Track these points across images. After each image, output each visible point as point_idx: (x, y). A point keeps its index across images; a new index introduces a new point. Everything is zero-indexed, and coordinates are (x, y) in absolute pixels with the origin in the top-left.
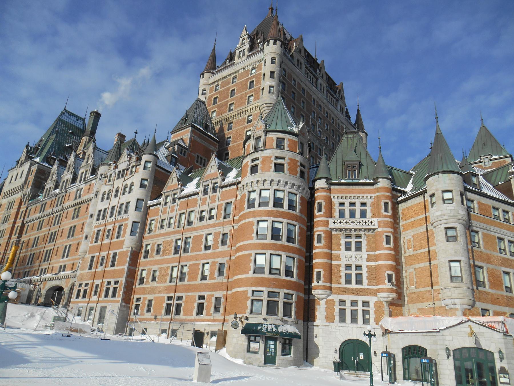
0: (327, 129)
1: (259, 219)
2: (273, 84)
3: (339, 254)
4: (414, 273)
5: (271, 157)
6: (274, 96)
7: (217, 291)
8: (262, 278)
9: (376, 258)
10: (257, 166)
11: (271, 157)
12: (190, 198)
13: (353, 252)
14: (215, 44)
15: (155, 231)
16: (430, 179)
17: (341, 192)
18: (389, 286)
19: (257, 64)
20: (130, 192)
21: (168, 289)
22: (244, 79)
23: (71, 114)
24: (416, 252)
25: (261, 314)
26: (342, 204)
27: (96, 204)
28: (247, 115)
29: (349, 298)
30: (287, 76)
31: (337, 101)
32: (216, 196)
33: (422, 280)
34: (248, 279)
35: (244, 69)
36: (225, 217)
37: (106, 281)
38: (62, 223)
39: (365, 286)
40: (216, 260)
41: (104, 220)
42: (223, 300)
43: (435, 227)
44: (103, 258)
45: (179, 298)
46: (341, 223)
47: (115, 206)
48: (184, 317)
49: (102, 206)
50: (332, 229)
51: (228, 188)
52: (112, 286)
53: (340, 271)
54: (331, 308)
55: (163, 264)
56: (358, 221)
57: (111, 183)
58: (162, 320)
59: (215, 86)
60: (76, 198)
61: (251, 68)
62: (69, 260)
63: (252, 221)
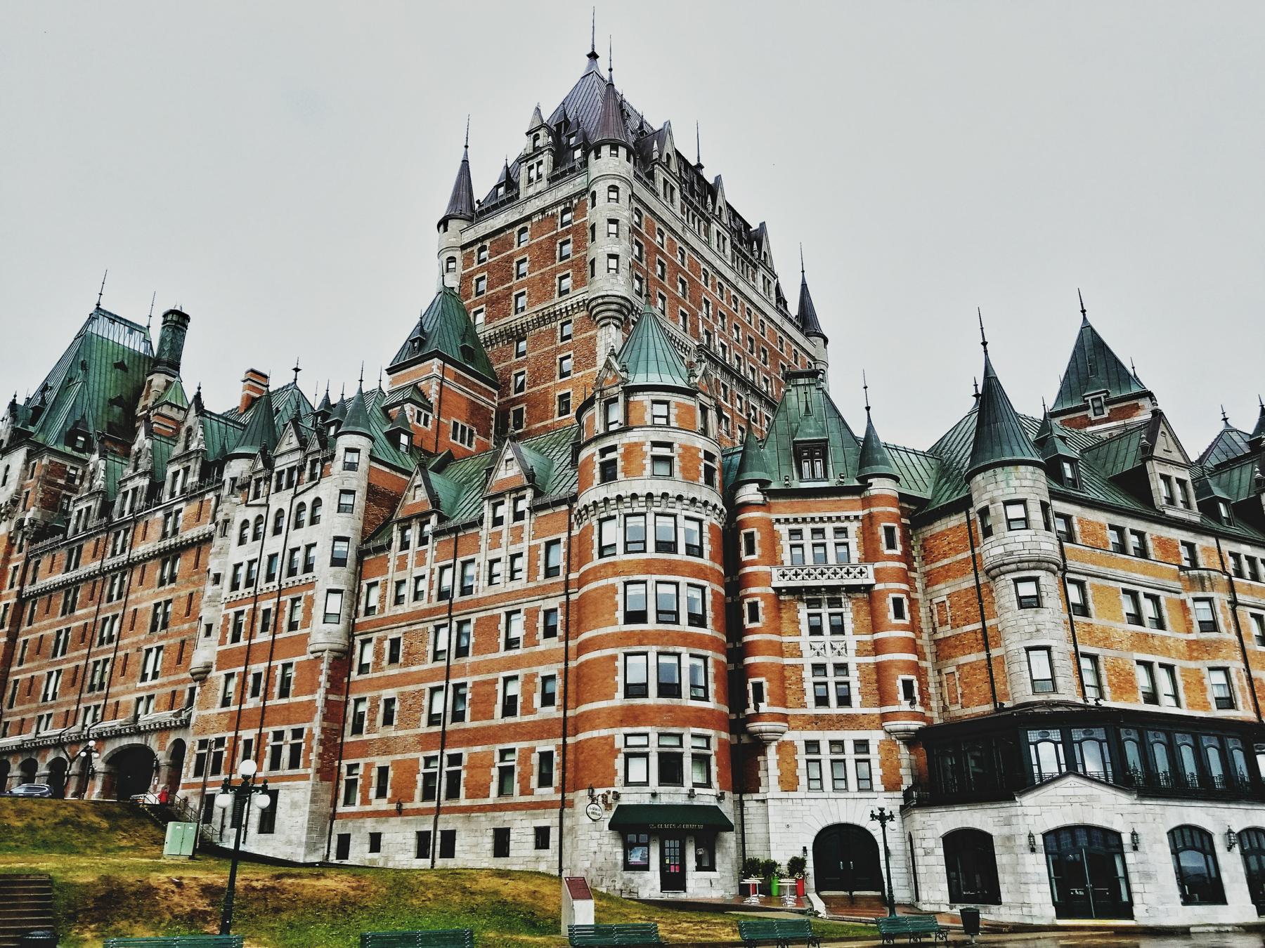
0: (738, 341)
1: (625, 579)
2: (615, 250)
3: (798, 643)
4: (957, 675)
5: (643, 444)
6: (619, 277)
7: (542, 738)
8: (644, 706)
9: (878, 647)
10: (614, 461)
11: (643, 444)
13: (827, 637)
14: (466, 147)
15: (383, 609)
16: (979, 477)
18: (905, 706)
20: (314, 520)
21: (425, 742)
23: (114, 319)
24: (958, 631)
25: (647, 784)
27: (222, 551)
28: (560, 322)
29: (824, 737)
30: (643, 226)
31: (755, 267)
32: (522, 527)
33: (974, 689)
34: (612, 710)
35: (543, 211)
36: (547, 575)
37: (269, 731)
38: (132, 597)
39: (856, 708)
41: (251, 589)
42: (557, 759)
43: (993, 578)
44: (257, 677)
45: (455, 760)
46: (796, 575)
47: (276, 555)
49: (242, 554)
50: (778, 590)
52: (286, 743)
53: (802, 680)
54: (789, 761)
55: (409, 684)
56: (832, 570)
57: (261, 500)
58: (418, 812)
59: (475, 251)
60: (164, 536)
62: (163, 685)
63: (613, 585)
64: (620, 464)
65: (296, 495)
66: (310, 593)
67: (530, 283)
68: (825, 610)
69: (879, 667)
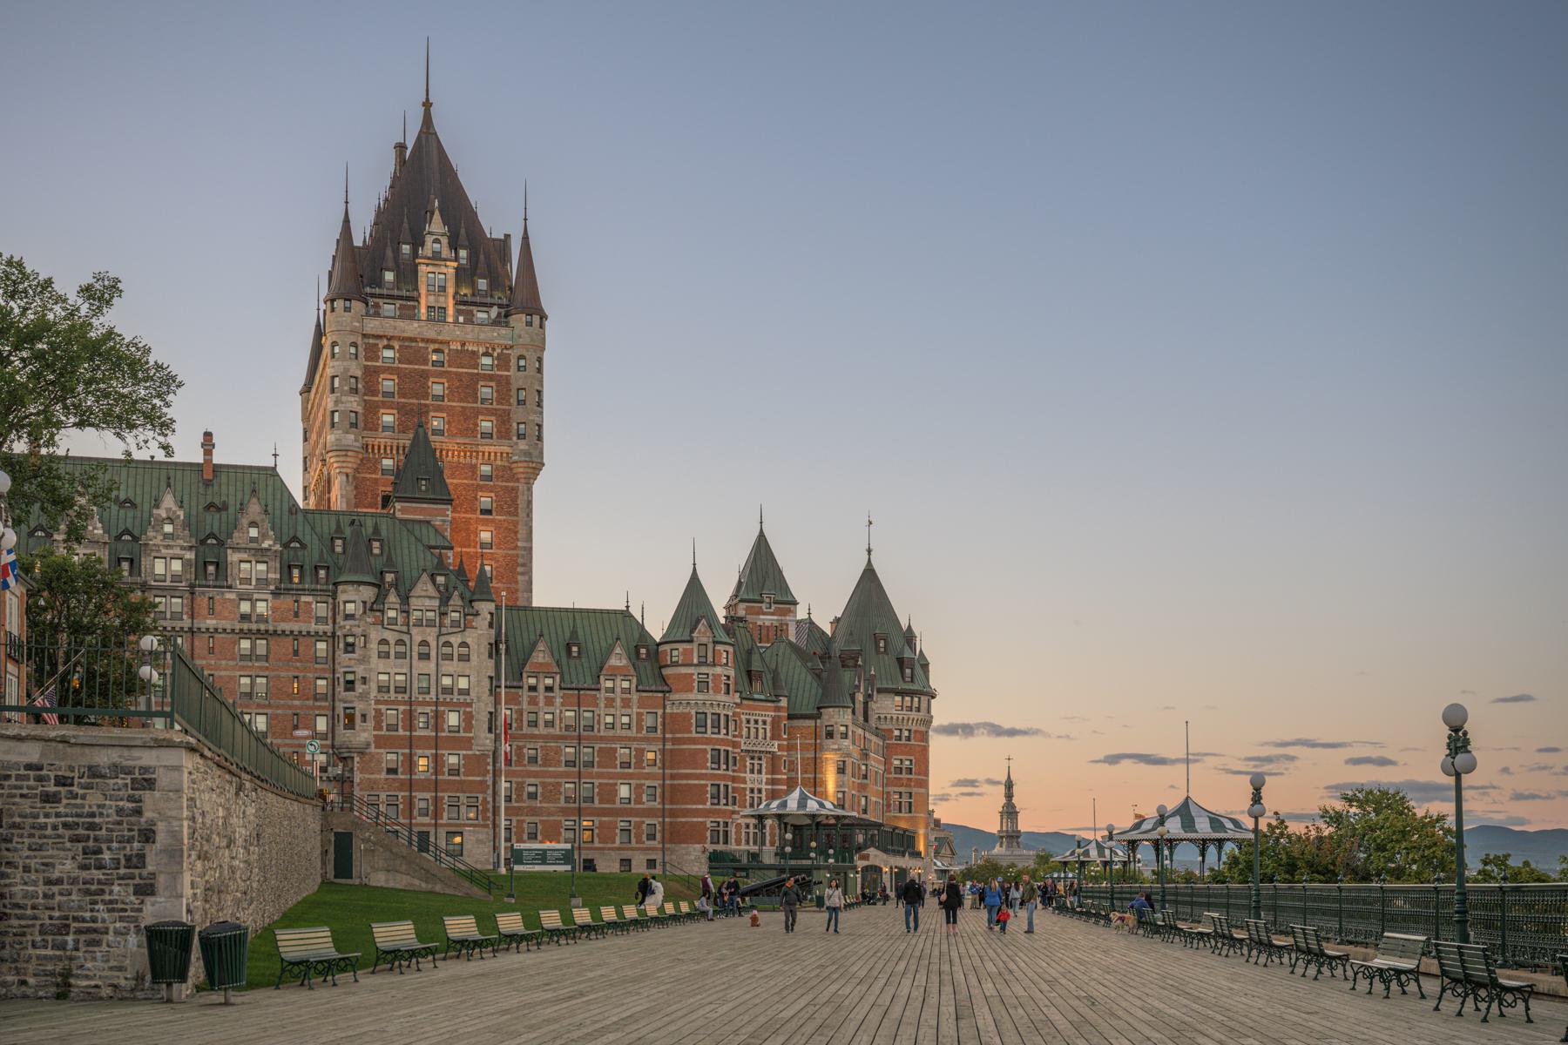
12: (582, 692)
13: (755, 776)
16: (831, 710)
17: (748, 707)
19: (499, 350)
21: (564, 812)
22: (466, 370)
26: (748, 722)
27: (364, 660)
40: (643, 782)
42: (658, 827)
48: (601, 845)
51: (650, 694)
52: (463, 804)
61: (481, 352)
64: (711, 685)
65: (440, 634)
66: (468, 709)
67: (449, 410)
68: (756, 762)
69: (773, 790)
